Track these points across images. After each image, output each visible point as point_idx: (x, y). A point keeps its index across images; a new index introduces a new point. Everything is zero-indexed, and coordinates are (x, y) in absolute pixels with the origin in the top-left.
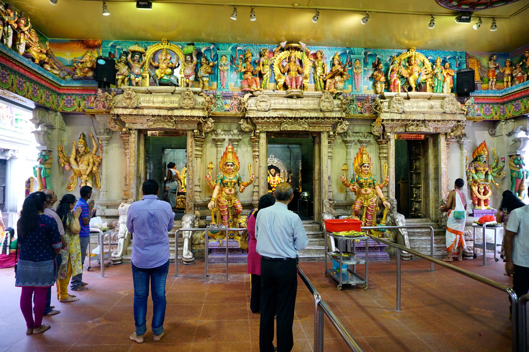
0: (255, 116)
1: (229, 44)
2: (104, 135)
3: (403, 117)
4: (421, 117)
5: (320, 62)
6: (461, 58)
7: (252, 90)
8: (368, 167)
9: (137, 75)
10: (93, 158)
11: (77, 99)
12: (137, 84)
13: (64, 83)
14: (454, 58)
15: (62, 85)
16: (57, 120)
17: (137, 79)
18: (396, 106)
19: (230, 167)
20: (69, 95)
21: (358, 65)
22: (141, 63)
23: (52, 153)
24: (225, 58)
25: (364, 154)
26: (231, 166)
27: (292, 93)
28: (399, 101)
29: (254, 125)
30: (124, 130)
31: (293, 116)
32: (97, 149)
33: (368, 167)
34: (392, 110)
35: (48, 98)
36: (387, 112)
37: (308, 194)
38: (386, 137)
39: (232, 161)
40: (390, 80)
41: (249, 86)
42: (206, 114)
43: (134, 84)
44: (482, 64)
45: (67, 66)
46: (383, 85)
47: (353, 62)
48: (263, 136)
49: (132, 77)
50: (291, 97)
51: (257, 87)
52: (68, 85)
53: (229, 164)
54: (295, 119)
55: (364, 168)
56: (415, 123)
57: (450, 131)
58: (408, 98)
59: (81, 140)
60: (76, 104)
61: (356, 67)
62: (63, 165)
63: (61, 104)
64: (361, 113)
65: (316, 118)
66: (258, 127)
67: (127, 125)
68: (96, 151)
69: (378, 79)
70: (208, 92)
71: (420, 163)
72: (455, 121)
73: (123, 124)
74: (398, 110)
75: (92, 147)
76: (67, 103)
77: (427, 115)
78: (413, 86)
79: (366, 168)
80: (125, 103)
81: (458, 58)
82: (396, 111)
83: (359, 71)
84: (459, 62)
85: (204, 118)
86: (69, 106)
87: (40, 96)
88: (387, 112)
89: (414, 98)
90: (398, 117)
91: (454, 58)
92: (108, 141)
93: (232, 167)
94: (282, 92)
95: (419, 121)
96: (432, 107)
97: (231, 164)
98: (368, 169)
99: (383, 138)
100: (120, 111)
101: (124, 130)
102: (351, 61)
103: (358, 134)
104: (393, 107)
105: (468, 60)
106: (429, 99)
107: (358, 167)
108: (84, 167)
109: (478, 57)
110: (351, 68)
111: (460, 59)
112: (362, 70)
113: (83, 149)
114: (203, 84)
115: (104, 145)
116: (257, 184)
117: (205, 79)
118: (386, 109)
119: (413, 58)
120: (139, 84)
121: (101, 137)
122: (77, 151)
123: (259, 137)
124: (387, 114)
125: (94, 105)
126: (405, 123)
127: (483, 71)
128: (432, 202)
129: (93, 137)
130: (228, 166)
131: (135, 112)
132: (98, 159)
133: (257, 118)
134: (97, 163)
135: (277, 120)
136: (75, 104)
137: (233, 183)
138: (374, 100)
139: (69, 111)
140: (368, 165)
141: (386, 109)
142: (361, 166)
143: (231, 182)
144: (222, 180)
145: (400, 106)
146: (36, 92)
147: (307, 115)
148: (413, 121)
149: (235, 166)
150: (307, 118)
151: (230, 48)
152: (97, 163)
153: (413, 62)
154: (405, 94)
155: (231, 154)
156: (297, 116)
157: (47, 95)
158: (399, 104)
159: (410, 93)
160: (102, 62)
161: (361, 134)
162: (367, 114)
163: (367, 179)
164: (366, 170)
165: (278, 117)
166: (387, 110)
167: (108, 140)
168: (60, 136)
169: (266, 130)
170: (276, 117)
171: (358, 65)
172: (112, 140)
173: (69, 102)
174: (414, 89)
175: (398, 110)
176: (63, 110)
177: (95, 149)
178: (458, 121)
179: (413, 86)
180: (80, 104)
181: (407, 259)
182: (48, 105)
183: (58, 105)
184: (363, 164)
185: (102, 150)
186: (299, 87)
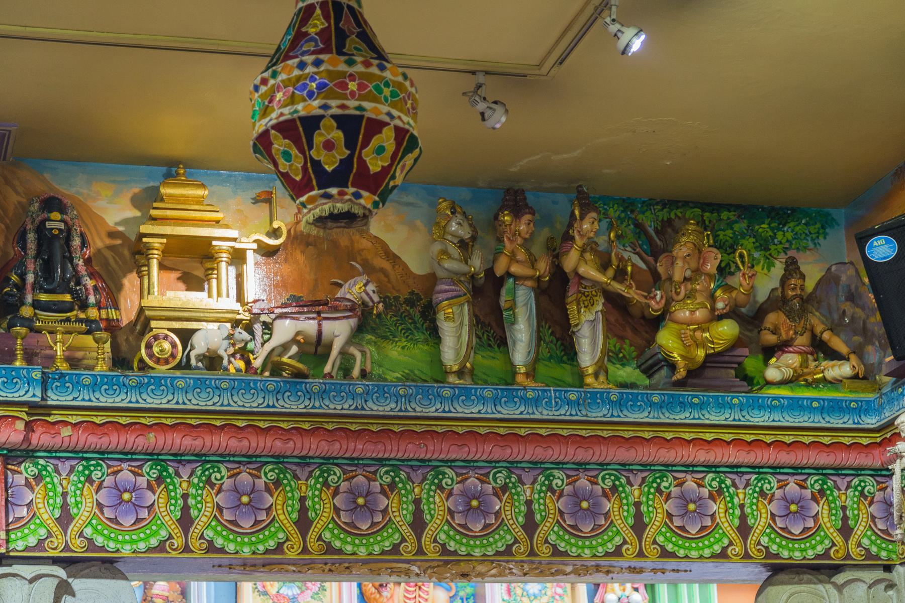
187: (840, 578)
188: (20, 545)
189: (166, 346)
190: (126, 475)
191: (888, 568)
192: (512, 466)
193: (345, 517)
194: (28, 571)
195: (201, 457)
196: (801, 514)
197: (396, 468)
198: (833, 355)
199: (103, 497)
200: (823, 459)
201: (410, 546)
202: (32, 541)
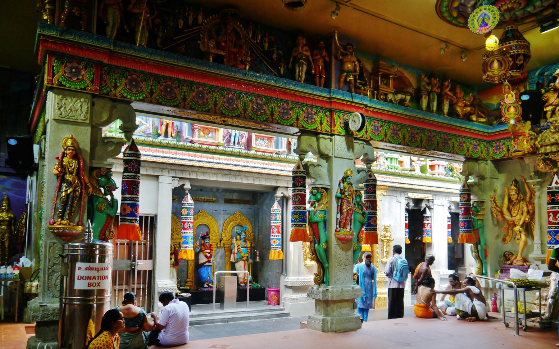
2: (535, 179)
10: (527, 206)
11: (506, 143)
13: (492, 129)
15: (490, 131)
16: (488, 167)
20: (497, 140)
23: (485, 204)
35: (476, 148)
45: (495, 110)
52: (495, 130)
59: (513, 187)
60: (505, 149)
62: (495, 216)
63: (491, 152)
75: (525, 194)
76: (497, 149)
80: (553, 138)
86: (498, 152)
87: (466, 149)
92: (540, 185)
100: (549, 149)
108: (518, 217)
113: (516, 196)
115: (536, 189)
122: (510, 200)
136: (504, 149)
139: (498, 158)
146: (462, 146)
157: (474, 145)
168: (491, 184)
173: (498, 148)
176: (493, 158)
180: (508, 148)
182: (476, 156)
183: (488, 154)
187: (480, 162)
188: (359, 136)
189: (382, 97)
190: (376, 123)
191: (486, 161)
192: (452, 135)
193: (373, 131)
194: (360, 142)
195: (389, 122)
196: (476, 148)
197: (418, 129)
198: (482, 117)
199: (372, 127)
200: (480, 138)
201: (420, 146)
202: (361, 136)
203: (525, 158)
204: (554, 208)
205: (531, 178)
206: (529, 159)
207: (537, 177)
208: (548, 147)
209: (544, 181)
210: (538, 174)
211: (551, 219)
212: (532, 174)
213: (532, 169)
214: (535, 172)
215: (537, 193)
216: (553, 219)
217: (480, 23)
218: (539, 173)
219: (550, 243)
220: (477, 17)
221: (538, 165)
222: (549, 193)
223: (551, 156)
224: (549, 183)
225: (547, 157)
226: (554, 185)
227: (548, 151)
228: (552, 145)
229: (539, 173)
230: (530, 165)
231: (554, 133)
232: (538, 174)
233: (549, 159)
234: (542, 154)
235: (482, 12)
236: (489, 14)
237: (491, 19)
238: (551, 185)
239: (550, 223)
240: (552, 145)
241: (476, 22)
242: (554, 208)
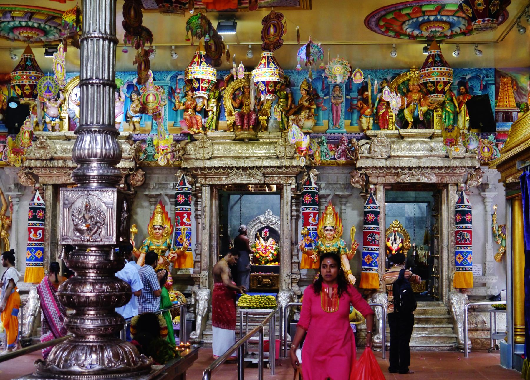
0: (192, 166)
1: (168, 72)
2: (14, 191)
3: (389, 163)
4: (414, 163)
5: (282, 93)
6: (487, 77)
7: (191, 133)
8: (331, 230)
9: (53, 117)
12: (53, 129)
14: (477, 77)
17: (53, 122)
18: (379, 150)
19: (157, 231)
21: (337, 93)
22: (59, 102)
24: (162, 90)
25: (328, 214)
26: (159, 229)
27: (241, 137)
28: (382, 142)
29: (194, 176)
30: (37, 185)
31: (241, 166)
32: (7, 207)
33: (331, 230)
34: (374, 154)
36: (368, 158)
37: (335, 273)
38: (369, 190)
39: (159, 224)
40: (377, 112)
41: (189, 128)
42: (132, 165)
43: (50, 128)
44: (520, 85)
46: (371, 119)
47: (331, 88)
48: (206, 191)
49: (48, 120)
50: (242, 140)
51: (198, 129)
53: (156, 227)
54: (244, 169)
55: (326, 232)
56: (406, 171)
57: (462, 180)
58: (401, 137)
61: (335, 95)
64: (335, 159)
65: (271, 167)
66: (199, 180)
67: (41, 180)
68: (6, 211)
69: (362, 111)
70: (139, 135)
71: (438, 224)
72: (464, 167)
73: (36, 178)
74: (382, 155)
77: (423, 160)
78: (410, 119)
79: (329, 232)
80: (38, 153)
81: (483, 78)
82: (380, 157)
83: (340, 101)
84: (484, 83)
85: (131, 169)
88: (368, 158)
89: (409, 137)
90: (382, 163)
91: (477, 77)
92: (19, 198)
93: (161, 231)
94: (231, 134)
95: (412, 168)
96: (432, 149)
97: (159, 227)
98: (332, 233)
99: (367, 191)
100: (33, 164)
101: (37, 185)
102: (328, 87)
103: (335, 186)
104: (375, 152)
105: (498, 80)
106: (431, 138)
107: (322, 230)
109: (514, 74)
110: (327, 97)
111: (486, 79)
112: (344, 99)
114: (134, 125)
115: (14, 203)
116: (199, 253)
117: (135, 119)
118: (366, 154)
119: (411, 83)
120: (56, 128)
121: (10, 194)
123: (201, 191)
124: (368, 161)
125: (3, 156)
126: (397, 171)
127: (521, 94)
128: (445, 280)
129: (2, 193)
130: (155, 229)
131: (49, 164)
132: (8, 221)
133: (196, 169)
134: (6, 226)
135: (221, 171)
137: (160, 251)
138: (350, 142)
140: (331, 228)
141: (366, 154)
142: (324, 229)
143: (159, 250)
144: (148, 247)
145: (384, 150)
147: (259, 163)
148: (403, 168)
149: (166, 229)
150: (259, 168)
151: (169, 77)
152: (6, 226)
153: (411, 87)
154: (396, 132)
155: (159, 215)
156: (246, 165)
158: (382, 146)
159: (402, 131)
160: (13, 105)
161: (338, 186)
162: (343, 160)
163: (329, 247)
164: (329, 235)
165: (222, 167)
166: (369, 155)
167: (20, 197)
169: (211, 183)
170: (219, 167)
171: (337, 93)
172: (24, 196)
174: (410, 124)
175: (382, 155)
177: (4, 208)
178: (471, 167)
179: (410, 119)
181: (378, 349)
184: (325, 227)
185: (12, 210)
186: (251, 127)
203: (5, 168)
204: (35, 224)
205: (10, 190)
206: (10, 169)
207: (17, 189)
208: (33, 161)
209: (23, 195)
210: (19, 186)
211: (32, 236)
212: (13, 186)
213: (12, 181)
214: (15, 184)
215: (15, 207)
216: (33, 236)
217: (46, 89)
218: (19, 186)
219: (29, 260)
220: (43, 84)
221: (20, 177)
222: (30, 208)
223: (35, 172)
224: (31, 198)
225: (31, 171)
226: (36, 201)
227: (32, 165)
228: (37, 159)
229: (19, 187)
230: (11, 176)
231: (40, 148)
232: (19, 186)
233: (32, 174)
234: (26, 167)
235: (47, 81)
236: (53, 84)
237: (54, 88)
238: (33, 200)
239: (30, 239)
240: (37, 159)
241: (42, 88)
242: (35, 224)
